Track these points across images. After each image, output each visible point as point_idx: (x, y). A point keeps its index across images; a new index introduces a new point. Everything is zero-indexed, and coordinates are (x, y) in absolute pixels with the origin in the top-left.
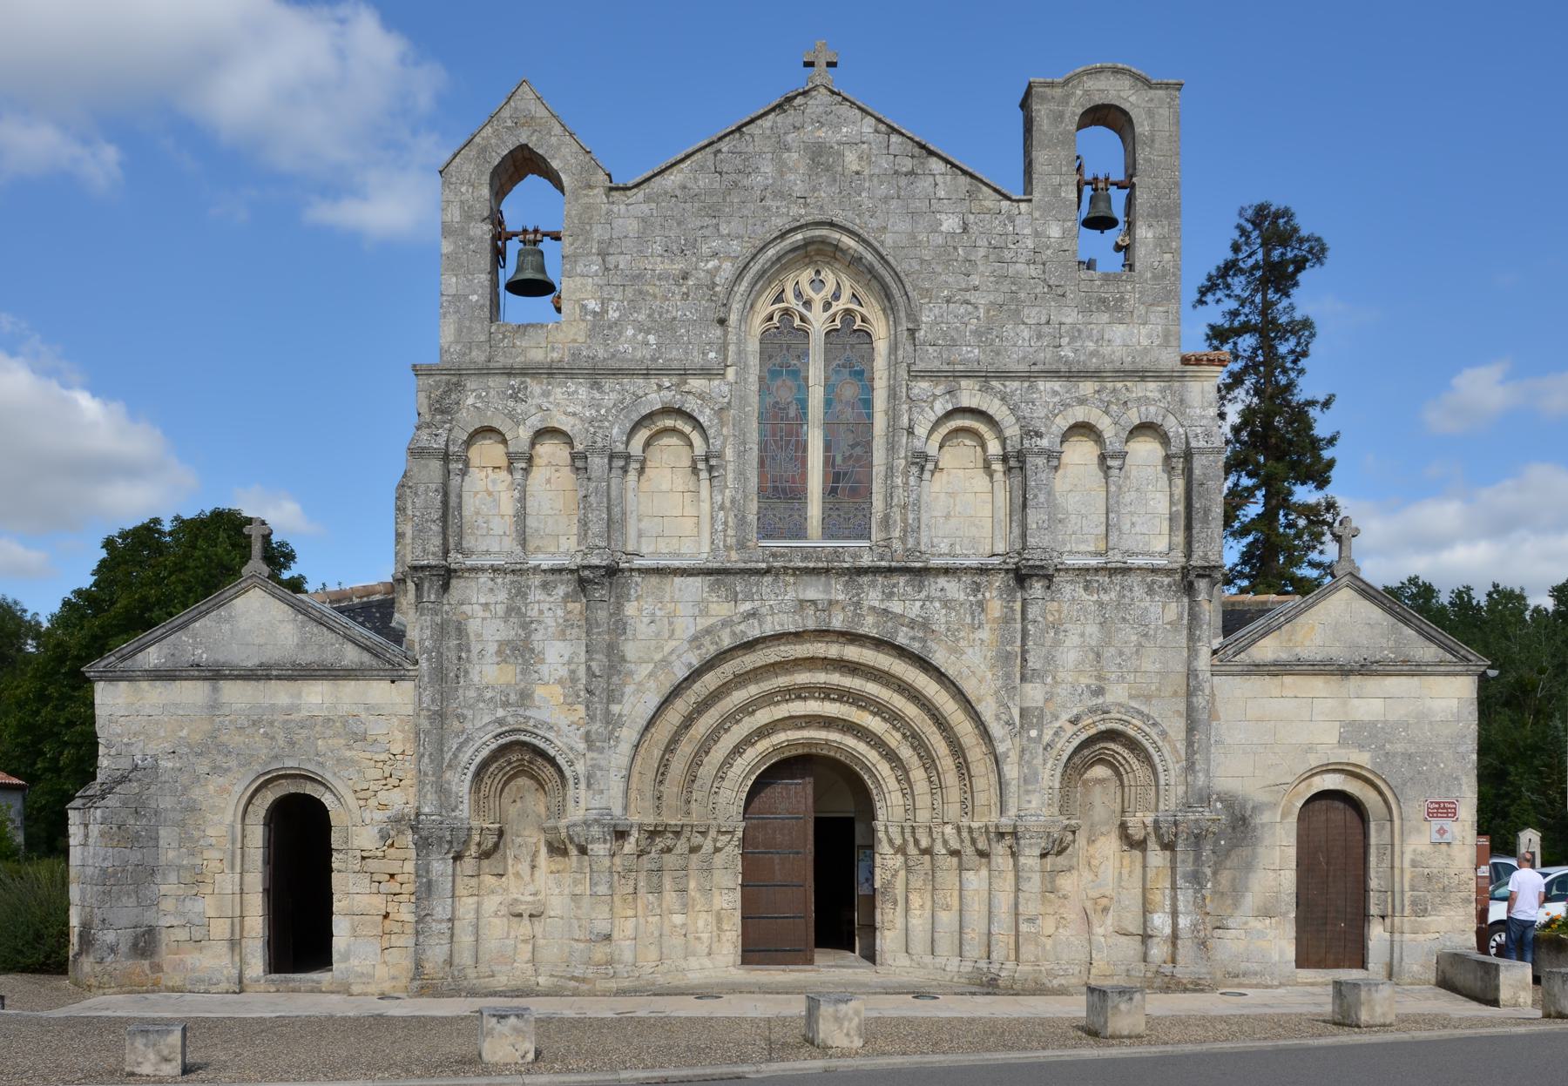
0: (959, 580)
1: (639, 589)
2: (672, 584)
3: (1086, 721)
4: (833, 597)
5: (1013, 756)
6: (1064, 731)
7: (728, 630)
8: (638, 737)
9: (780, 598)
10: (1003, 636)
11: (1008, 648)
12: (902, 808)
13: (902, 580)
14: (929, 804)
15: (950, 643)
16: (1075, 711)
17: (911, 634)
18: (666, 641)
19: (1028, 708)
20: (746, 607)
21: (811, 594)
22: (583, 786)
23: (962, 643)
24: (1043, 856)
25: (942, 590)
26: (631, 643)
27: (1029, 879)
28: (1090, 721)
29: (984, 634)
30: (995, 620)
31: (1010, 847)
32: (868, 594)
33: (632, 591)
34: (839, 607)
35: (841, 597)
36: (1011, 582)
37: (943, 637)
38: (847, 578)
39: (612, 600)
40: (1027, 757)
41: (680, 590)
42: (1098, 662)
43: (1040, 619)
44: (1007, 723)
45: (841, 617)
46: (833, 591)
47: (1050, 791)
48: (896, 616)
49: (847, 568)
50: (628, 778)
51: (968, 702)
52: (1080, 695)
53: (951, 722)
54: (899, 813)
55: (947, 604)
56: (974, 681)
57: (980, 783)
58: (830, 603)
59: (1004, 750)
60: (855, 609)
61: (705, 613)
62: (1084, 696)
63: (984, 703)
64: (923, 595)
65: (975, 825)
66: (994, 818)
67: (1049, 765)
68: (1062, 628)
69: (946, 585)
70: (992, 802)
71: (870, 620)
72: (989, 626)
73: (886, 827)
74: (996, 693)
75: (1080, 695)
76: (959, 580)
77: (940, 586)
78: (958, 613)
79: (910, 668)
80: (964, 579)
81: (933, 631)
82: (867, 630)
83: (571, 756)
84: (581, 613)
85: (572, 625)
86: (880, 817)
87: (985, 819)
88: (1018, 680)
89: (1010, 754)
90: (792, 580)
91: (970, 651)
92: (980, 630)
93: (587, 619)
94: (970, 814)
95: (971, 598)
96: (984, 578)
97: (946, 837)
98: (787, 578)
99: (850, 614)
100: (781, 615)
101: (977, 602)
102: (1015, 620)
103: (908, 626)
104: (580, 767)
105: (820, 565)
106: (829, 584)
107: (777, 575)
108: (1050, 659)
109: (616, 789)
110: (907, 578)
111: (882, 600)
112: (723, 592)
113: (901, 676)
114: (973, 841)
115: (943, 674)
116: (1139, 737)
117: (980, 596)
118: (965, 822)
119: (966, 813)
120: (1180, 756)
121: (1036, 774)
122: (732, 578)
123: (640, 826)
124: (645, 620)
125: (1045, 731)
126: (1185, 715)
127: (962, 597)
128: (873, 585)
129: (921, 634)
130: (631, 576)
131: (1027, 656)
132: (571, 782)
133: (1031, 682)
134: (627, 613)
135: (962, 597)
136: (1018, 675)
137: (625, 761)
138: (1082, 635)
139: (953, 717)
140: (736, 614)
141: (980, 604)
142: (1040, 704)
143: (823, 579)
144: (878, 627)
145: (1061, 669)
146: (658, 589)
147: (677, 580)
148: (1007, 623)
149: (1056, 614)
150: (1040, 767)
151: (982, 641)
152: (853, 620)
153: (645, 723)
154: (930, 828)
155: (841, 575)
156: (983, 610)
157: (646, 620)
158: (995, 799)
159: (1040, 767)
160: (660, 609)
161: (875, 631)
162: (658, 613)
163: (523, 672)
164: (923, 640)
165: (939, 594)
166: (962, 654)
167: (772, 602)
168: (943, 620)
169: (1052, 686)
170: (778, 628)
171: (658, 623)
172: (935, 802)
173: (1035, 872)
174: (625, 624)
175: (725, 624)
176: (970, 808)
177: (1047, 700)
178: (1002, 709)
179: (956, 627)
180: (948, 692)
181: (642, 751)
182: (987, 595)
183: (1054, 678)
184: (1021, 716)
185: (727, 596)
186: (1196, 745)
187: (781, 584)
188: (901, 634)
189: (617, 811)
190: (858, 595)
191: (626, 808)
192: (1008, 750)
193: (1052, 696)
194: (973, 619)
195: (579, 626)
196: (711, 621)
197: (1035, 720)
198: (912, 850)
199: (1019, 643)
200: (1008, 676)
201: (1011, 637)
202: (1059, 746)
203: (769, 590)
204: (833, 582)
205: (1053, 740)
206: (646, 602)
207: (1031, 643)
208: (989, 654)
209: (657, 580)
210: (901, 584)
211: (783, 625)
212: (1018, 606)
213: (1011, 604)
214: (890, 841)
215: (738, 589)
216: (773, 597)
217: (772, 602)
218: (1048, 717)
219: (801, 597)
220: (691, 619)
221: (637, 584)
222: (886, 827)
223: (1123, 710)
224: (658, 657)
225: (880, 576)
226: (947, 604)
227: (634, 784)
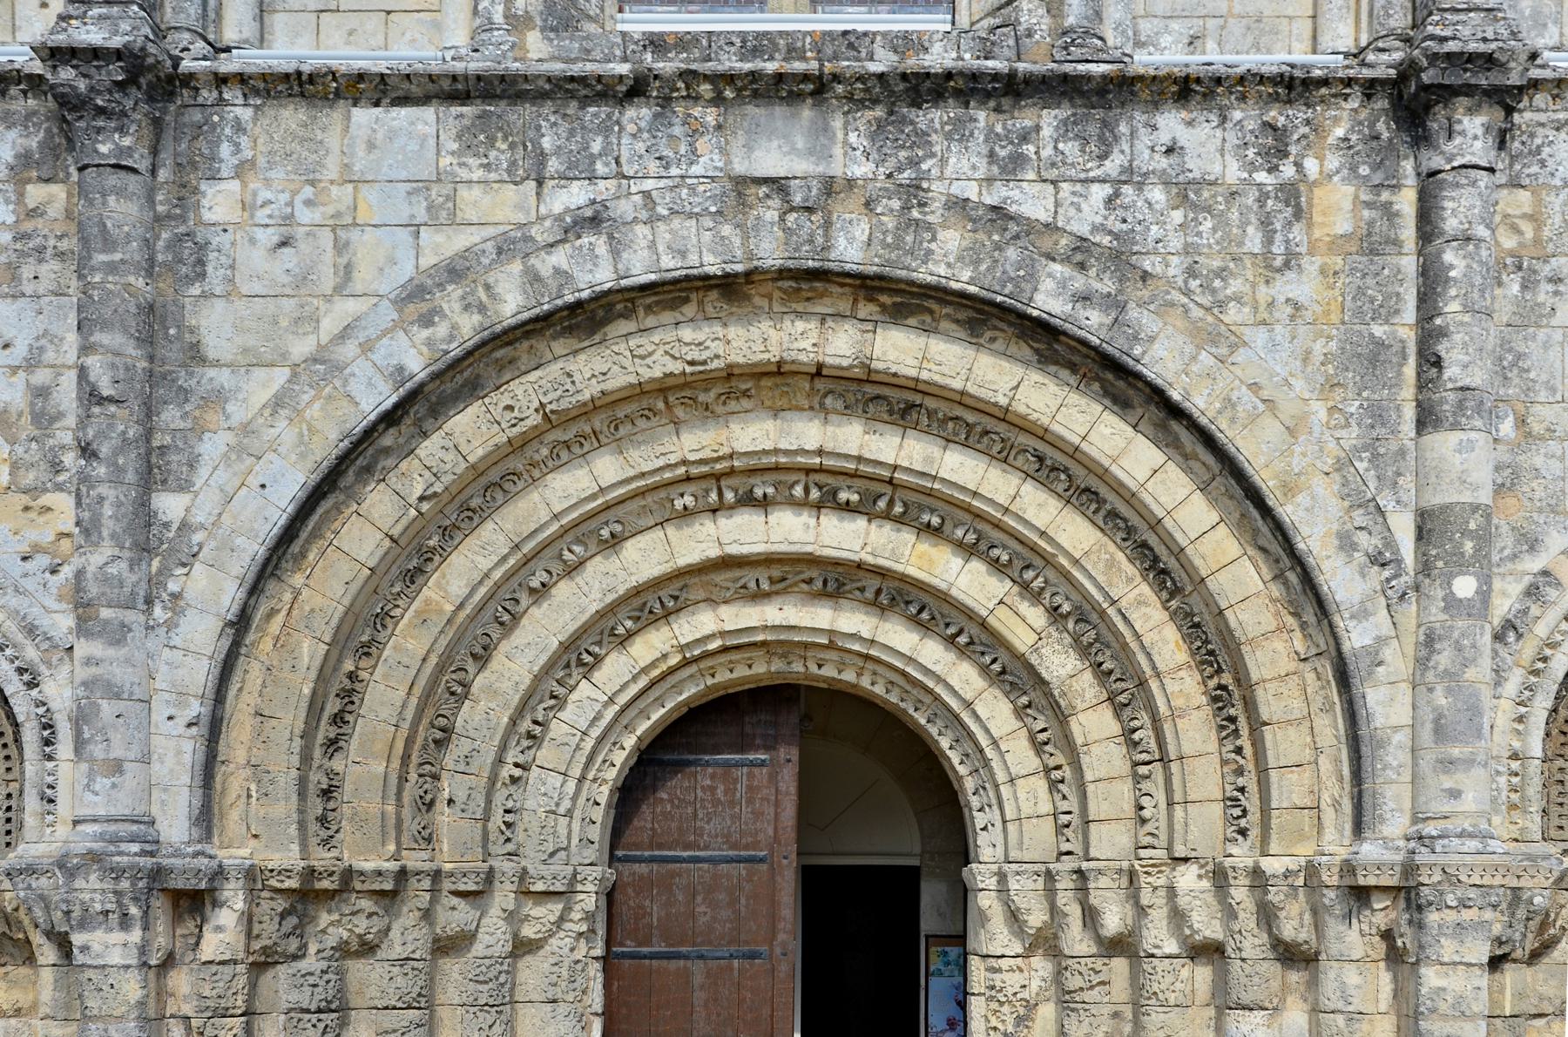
0: (1224, 119)
1: (244, 141)
2: (346, 129)
4: (836, 169)
5: (1397, 661)
6: (1558, 584)
7: (516, 267)
8: (241, 595)
9: (674, 171)
10: (1360, 291)
11: (1379, 330)
12: (1049, 824)
13: (1049, 120)
14: (1128, 809)
15: (1196, 312)
17: (1079, 283)
18: (328, 298)
19: (1446, 508)
20: (575, 196)
21: (770, 160)
22: (64, 749)
23: (1233, 314)
24: (1495, 963)
25: (1170, 151)
26: (219, 304)
29: (1303, 286)
30: (1336, 244)
31: (1387, 935)
32: (943, 162)
33: (225, 150)
34: (856, 200)
35: (861, 169)
36: (1381, 126)
37: (1175, 296)
38: (879, 112)
39: (163, 175)
40: (1444, 659)
41: (371, 146)
43: (1481, 231)
44: (1378, 561)
45: (861, 230)
46: (838, 151)
47: (1515, 765)
48: (1030, 228)
49: (881, 77)
50: (214, 728)
51: (1255, 496)
53: (1198, 562)
54: (1039, 839)
55: (1186, 191)
56: (1271, 430)
57: (1284, 744)
58: (830, 186)
59: (1368, 641)
60: (906, 208)
61: (446, 215)
63: (1302, 499)
64: (1113, 166)
65: (1272, 866)
66: (1335, 843)
67: (1512, 687)
68: (1546, 270)
69: (1185, 136)
70: (1326, 798)
71: (951, 240)
72: (1318, 260)
73: (1002, 877)
74: (1343, 464)
76: (1224, 119)
77: (1164, 138)
78: (1221, 221)
79: (1074, 398)
80: (1237, 115)
81: (1145, 276)
82: (942, 270)
83: (31, 653)
84: (69, 215)
85: (41, 250)
86: (986, 853)
87: (1306, 849)
88: (1408, 427)
89: (1388, 653)
90: (711, 116)
91: (1259, 337)
92: (1290, 275)
93: (81, 227)
94: (1254, 833)
95: (1261, 177)
96: (1299, 113)
97: (1182, 902)
98: (697, 111)
99: (889, 222)
100: (676, 222)
101: (1281, 187)
102: (1397, 243)
103: (1066, 260)
104: (59, 692)
105: (798, 66)
106: (826, 129)
107: (666, 101)
108: (1509, 363)
109: (170, 761)
110: (1064, 112)
111: (990, 180)
112: (501, 153)
113: (1045, 421)
114: (1267, 915)
115: (1176, 412)
117: (1288, 171)
118: (1242, 855)
119: (1243, 832)
121: (1474, 711)
122: (527, 111)
123: (252, 876)
124: (260, 234)
125: (1497, 584)
127: (1233, 172)
128: (959, 132)
129: (1107, 286)
130: (221, 101)
131: (1441, 348)
132: (30, 736)
133: (1455, 427)
134: (208, 216)
135: (1233, 172)
136: (1409, 412)
137: (199, 673)
139: (1206, 545)
140: (540, 219)
141: (1290, 194)
142: (1485, 497)
143: (807, 112)
144: (977, 263)
145: (1543, 396)
146: (303, 140)
147: (363, 116)
148: (1373, 252)
149: (1528, 230)
150: (1486, 693)
151: (1297, 307)
152: (899, 239)
153: (262, 552)
154: (1132, 875)
155: (861, 104)
156: (1298, 214)
157: (268, 237)
158: (1335, 791)
159: (1486, 693)
160: (309, 203)
161: (966, 275)
162: (305, 215)
164: (1115, 304)
165: (1163, 162)
166: (1233, 348)
167: (649, 185)
168: (1176, 243)
169: (1514, 449)
171: (303, 246)
172: (1145, 801)
173: (1472, 1017)
174: (202, 247)
175: (506, 248)
176: (1254, 816)
177: (1499, 489)
178: (1359, 518)
179: (1216, 264)
180: (1188, 471)
181: (262, 643)
182: (1311, 165)
183: (1521, 422)
184: (1421, 535)
185: (513, 163)
187: (677, 130)
188: (1047, 285)
189: (175, 827)
190: (914, 163)
191: (206, 818)
192: (1381, 641)
193: (1516, 475)
194: (1269, 240)
195: (60, 255)
196: (462, 240)
198: (1076, 941)
199: (1409, 314)
200: (1377, 415)
201: (1387, 297)
202: (1541, 630)
203: (640, 147)
204: (837, 123)
206: (268, 182)
207: (1454, 306)
208: (1319, 348)
209: (302, 115)
210: (1047, 132)
211: (683, 254)
212: (1406, 201)
213: (1385, 196)
214: (1014, 917)
215: (547, 143)
216: (653, 167)
217: (649, 185)
218: (1505, 541)
219: (740, 167)
220: (404, 235)
221: (239, 127)
222: (1002, 877)
225: (982, 103)
226: (1186, 191)
227: (238, 742)
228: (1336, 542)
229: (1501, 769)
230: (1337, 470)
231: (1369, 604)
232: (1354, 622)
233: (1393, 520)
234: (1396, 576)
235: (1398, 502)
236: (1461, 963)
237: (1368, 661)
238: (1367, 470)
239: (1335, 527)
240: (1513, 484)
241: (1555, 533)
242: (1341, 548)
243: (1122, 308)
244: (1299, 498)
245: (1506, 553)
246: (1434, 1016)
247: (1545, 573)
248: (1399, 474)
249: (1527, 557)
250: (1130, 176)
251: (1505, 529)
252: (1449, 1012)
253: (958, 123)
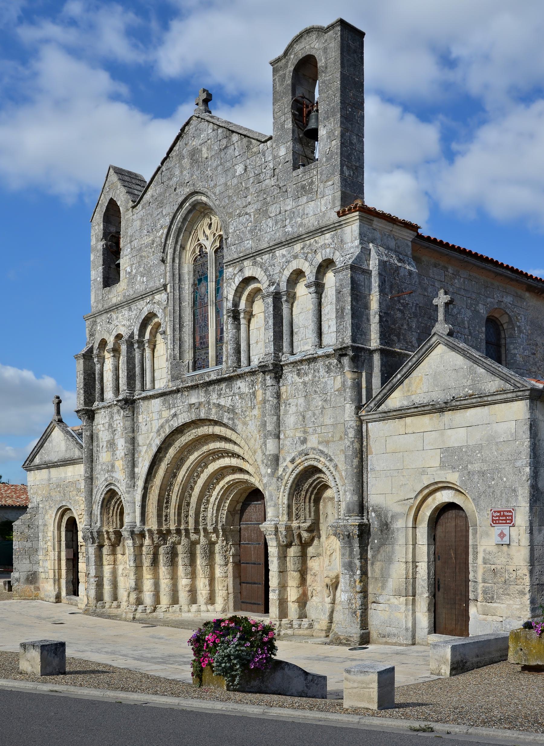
3: (298, 461)
23: (248, 419)
37: (240, 417)
38: (205, 389)
42: (304, 422)
45: (203, 411)
55: (241, 395)
62: (297, 445)
74: (261, 447)
75: (296, 444)
106: (199, 393)
129: (232, 416)
138: (297, 406)
163: (113, 455)
164: (233, 419)
168: (240, 406)
170: (183, 421)
194: (251, 404)
208: (258, 424)
223: (315, 452)
224: (148, 442)
226: (241, 395)
243: (234, 420)
247: (286, 466)
250: (234, 394)
253: (214, 389)
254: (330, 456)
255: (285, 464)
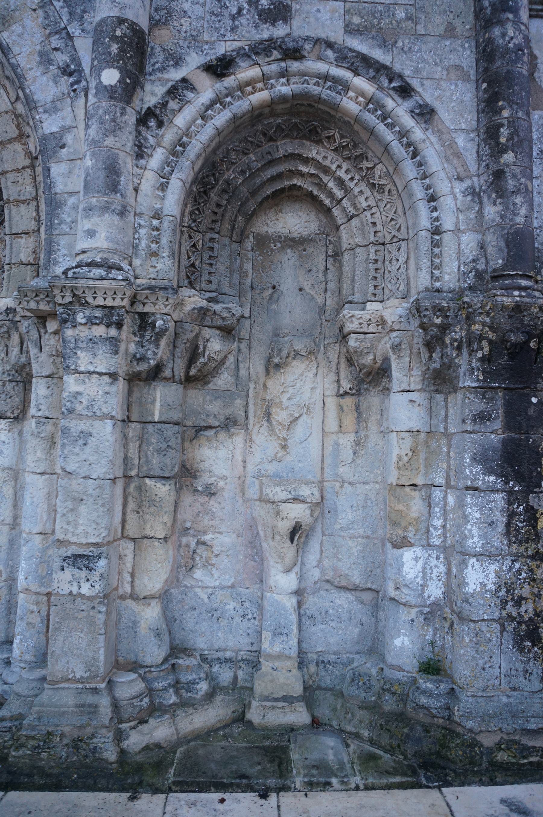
6: (193, 89)
16: (221, 49)
27: (86, 435)
28: (254, 72)
44: (66, 71)
47: (155, 222)
52: (234, 18)
59: (55, 129)
63: (17, 28)
75: (234, 18)
89: (69, 138)
116: (371, 119)
120: (467, 170)
125: (148, 87)
126: (473, 77)
173: (103, 417)
178: (55, 42)
186: (504, 131)
192: (65, 129)
193: (170, 14)
197: (115, 48)
205: (164, 105)
228: (38, 59)
229: (142, 222)
230: (41, 7)
231: (58, 103)
232: (47, 115)
233: (78, 43)
234: (77, 82)
235: (83, 30)
236: (94, 372)
237: (54, 143)
238: (62, 7)
239: (38, 48)
240: (167, 21)
241: (194, 55)
242: (41, 63)
244: (14, 27)
245: (157, 66)
246: (72, 416)
248: (85, 11)
249: (172, 69)
251: (158, 49)
252: (84, 412)
254: (400, 76)
255: (176, 75)
